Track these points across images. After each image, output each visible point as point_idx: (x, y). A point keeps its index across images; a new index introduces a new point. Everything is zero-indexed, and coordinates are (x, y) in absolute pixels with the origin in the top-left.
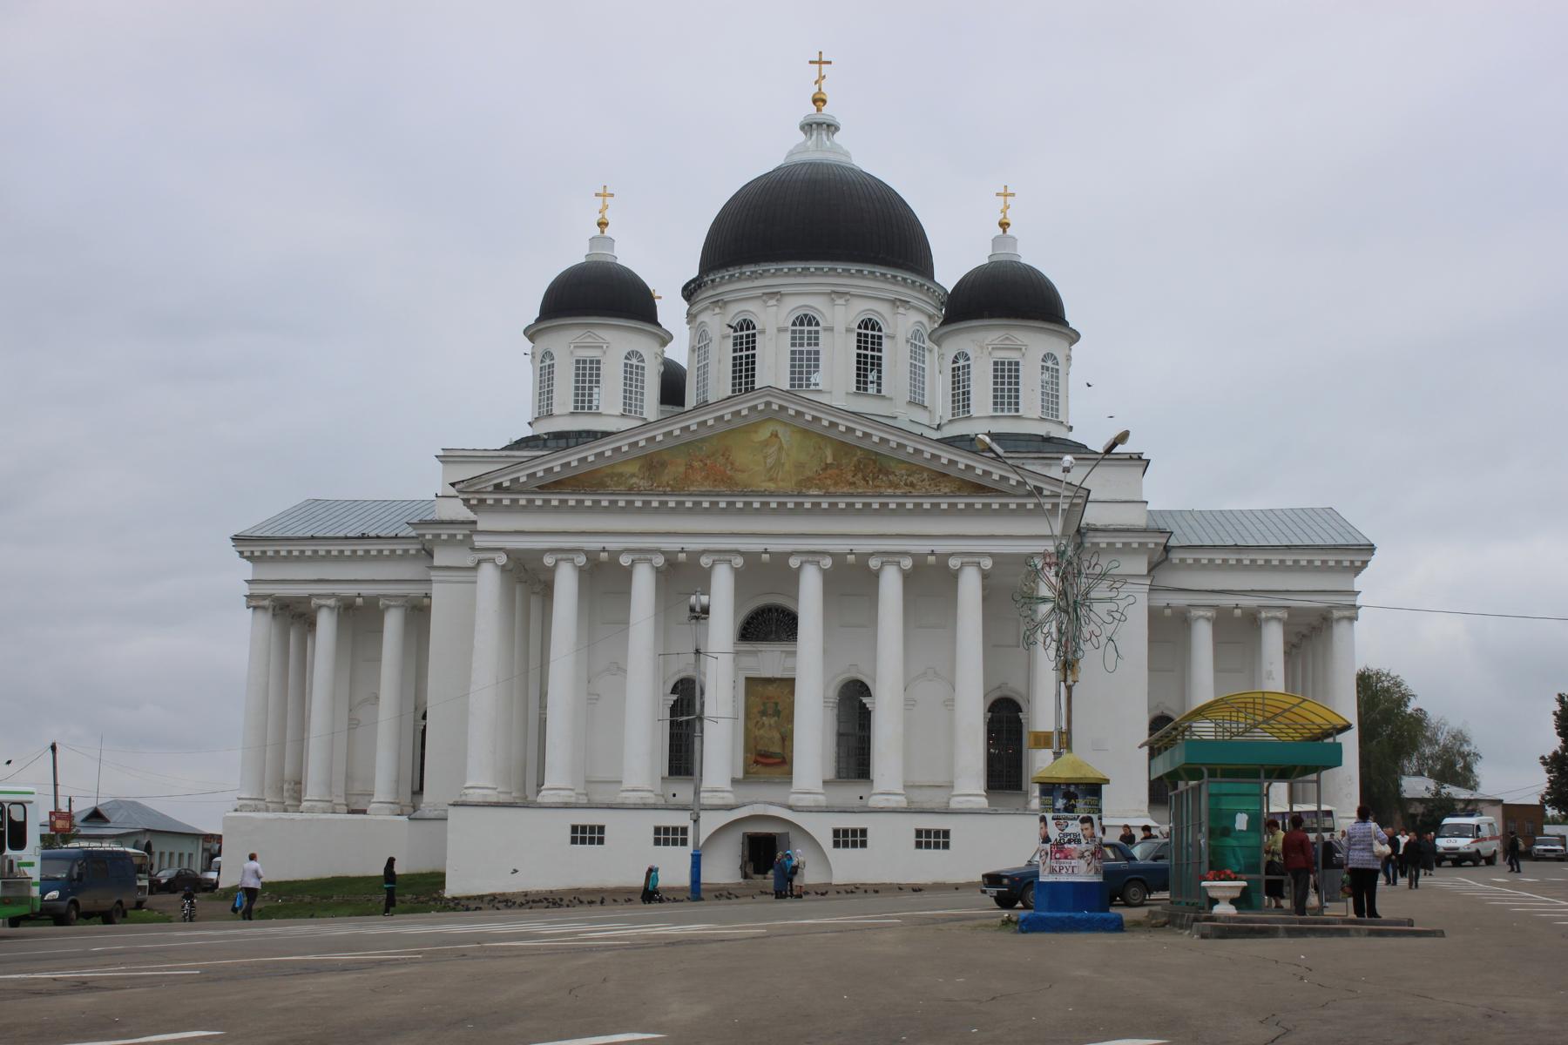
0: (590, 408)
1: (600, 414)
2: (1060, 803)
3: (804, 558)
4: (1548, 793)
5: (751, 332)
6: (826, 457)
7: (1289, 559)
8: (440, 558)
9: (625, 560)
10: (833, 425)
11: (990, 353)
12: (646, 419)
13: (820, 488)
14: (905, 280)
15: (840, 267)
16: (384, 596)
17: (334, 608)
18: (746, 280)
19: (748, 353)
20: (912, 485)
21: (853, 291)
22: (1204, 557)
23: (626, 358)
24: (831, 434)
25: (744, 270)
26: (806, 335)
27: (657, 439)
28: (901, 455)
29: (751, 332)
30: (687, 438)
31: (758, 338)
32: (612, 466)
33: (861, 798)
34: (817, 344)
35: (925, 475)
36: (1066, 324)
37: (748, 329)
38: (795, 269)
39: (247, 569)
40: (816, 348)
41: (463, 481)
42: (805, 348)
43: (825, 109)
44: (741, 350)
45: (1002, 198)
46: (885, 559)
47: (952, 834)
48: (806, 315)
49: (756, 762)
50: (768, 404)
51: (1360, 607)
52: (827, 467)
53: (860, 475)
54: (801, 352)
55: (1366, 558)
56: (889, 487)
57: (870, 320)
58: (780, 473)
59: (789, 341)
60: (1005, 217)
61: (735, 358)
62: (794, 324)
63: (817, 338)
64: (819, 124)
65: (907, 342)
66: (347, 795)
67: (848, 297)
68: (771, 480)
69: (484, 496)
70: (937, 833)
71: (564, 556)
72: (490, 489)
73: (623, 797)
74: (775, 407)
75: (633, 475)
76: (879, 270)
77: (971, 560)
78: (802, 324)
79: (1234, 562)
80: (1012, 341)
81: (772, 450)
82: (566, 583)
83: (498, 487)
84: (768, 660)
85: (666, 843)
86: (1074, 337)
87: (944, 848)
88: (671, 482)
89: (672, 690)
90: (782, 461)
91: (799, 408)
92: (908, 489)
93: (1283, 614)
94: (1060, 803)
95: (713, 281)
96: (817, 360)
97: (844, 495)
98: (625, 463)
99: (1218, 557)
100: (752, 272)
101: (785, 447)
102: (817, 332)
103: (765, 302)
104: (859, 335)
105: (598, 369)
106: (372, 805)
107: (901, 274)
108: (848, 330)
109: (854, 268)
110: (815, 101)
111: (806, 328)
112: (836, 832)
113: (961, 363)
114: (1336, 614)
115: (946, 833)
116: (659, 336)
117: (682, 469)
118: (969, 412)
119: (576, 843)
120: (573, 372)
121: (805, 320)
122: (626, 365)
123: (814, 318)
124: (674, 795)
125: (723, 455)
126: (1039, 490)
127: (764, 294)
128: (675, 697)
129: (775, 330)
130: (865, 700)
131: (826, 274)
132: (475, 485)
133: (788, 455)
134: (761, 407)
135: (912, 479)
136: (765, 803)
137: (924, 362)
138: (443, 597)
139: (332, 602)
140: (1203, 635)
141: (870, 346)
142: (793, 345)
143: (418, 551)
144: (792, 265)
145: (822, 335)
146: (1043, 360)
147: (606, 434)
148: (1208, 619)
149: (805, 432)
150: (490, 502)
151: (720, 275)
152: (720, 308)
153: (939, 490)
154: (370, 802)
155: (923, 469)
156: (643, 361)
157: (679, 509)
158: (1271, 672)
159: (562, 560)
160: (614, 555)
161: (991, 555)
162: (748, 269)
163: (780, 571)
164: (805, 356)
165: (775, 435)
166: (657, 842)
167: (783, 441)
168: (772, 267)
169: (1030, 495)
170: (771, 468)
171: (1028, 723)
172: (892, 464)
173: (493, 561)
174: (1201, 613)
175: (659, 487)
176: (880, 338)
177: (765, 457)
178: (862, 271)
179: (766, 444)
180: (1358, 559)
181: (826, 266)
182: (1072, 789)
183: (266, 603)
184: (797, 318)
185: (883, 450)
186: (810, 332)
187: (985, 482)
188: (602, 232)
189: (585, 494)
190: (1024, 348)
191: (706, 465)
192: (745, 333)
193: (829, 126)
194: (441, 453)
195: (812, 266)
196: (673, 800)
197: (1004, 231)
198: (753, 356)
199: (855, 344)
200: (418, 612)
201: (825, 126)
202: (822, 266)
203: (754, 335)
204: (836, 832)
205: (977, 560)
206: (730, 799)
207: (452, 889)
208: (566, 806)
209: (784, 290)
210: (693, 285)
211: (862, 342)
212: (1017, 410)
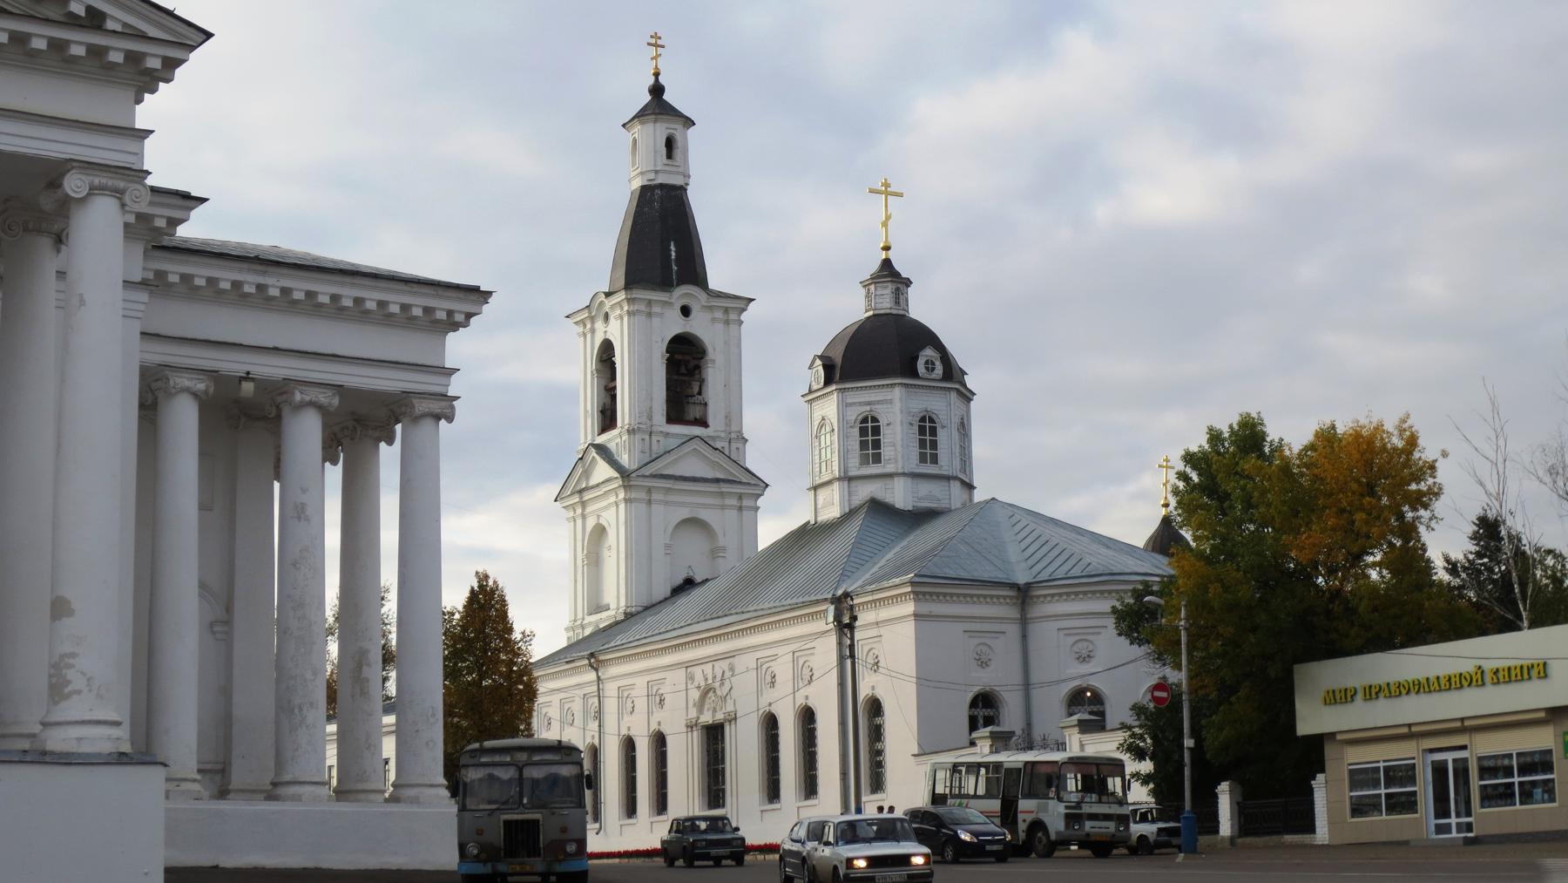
79: (252, 290)
93: (332, 400)
99: (226, 276)
114: (421, 406)
148: (195, 395)
158: (303, 505)
169: (73, 21)
174: (184, 381)
180: (460, 306)
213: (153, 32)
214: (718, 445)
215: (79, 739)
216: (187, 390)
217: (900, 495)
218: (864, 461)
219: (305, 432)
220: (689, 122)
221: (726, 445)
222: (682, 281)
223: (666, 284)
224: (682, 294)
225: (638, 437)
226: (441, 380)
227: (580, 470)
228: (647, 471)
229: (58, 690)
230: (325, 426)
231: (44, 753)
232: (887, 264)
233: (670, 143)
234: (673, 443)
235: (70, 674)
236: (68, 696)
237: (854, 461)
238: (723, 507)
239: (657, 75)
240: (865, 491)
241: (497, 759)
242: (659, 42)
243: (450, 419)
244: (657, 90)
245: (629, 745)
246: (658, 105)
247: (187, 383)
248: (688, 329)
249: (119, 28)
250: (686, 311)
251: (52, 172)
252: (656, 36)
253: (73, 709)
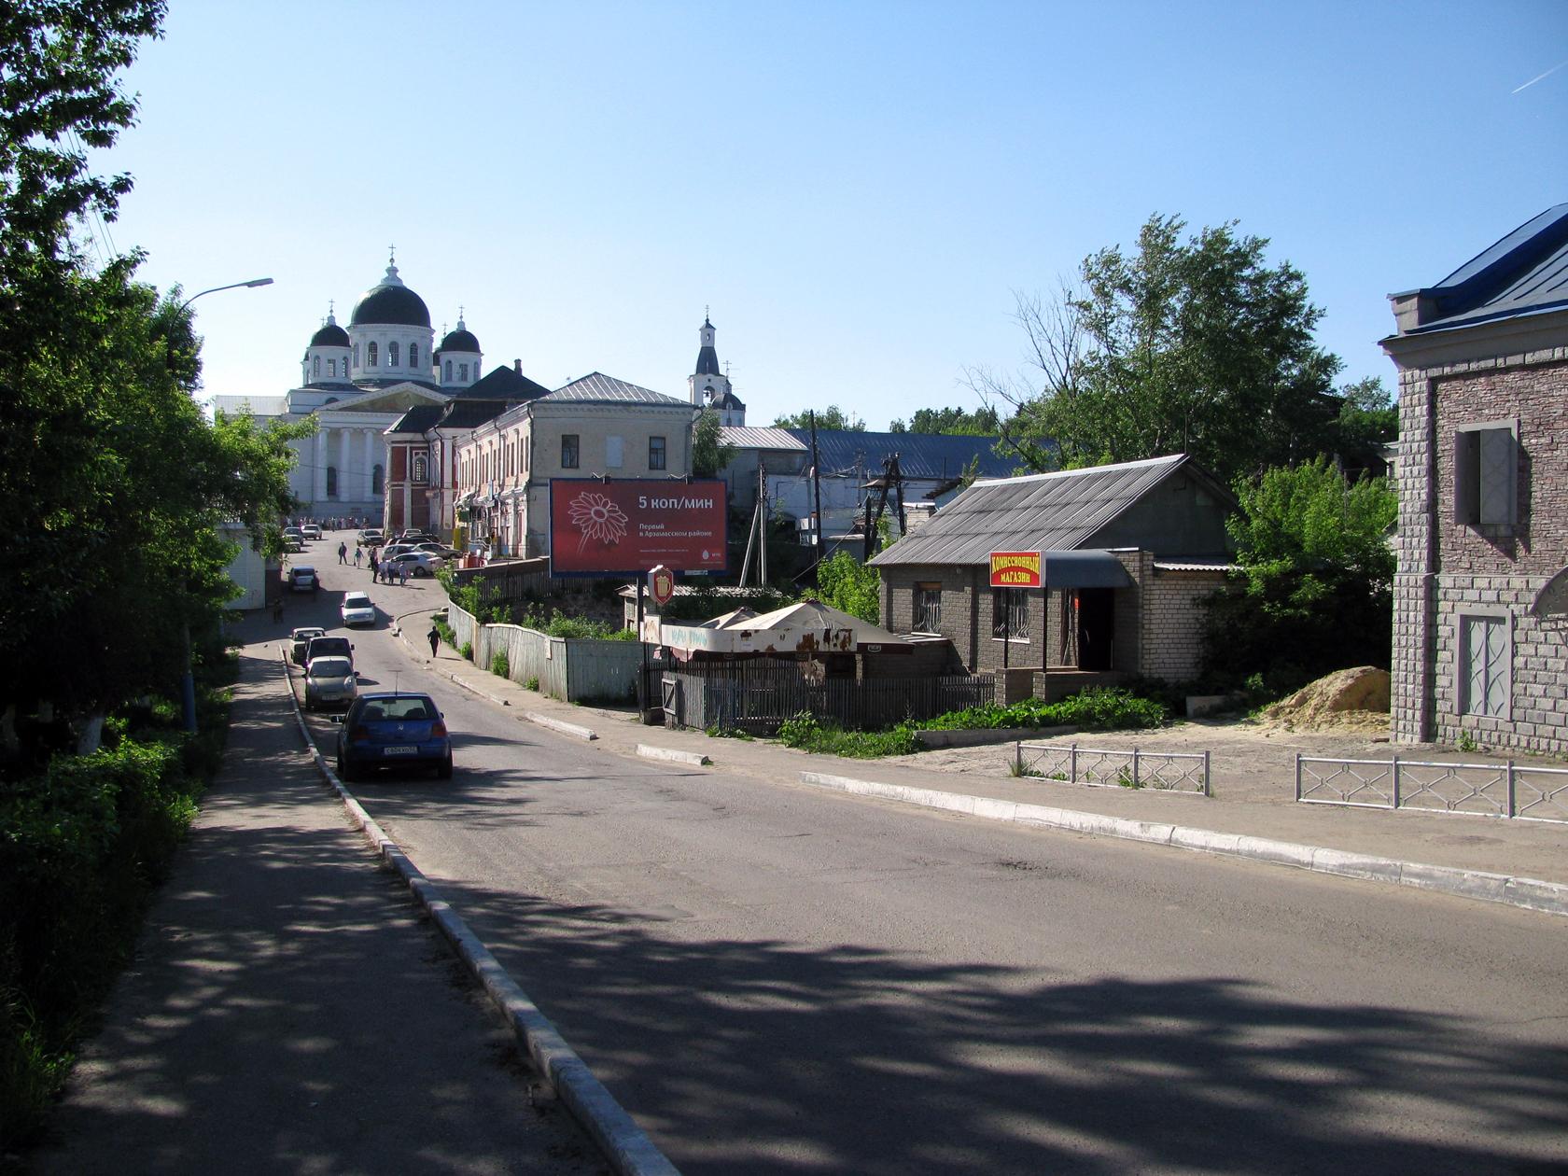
73: (365, 500)
81: (407, 399)
149: (417, 395)
160: (362, 430)
168: (383, 325)
244: (707, 320)
246: (708, 325)
250: (709, 380)
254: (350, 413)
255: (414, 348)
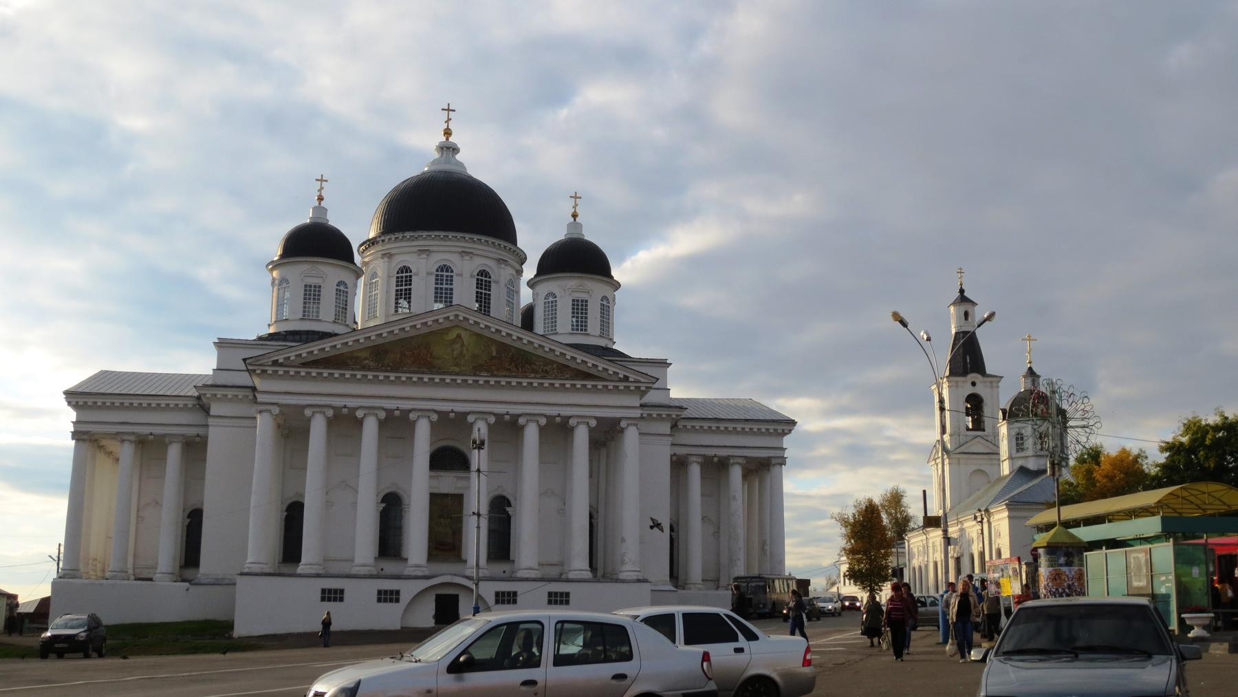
0: (309, 316)
1: (320, 320)
2: (1062, 560)
3: (477, 416)
4: (847, 571)
5: (408, 274)
6: (492, 352)
7: (747, 427)
8: (214, 410)
9: (359, 414)
10: (498, 331)
11: (570, 294)
12: (348, 325)
13: (488, 373)
14: (505, 247)
15: (468, 236)
16: (168, 434)
17: (133, 442)
18: (406, 241)
19: (406, 287)
20: (547, 372)
21: (476, 252)
22: (697, 424)
23: (337, 285)
24: (497, 337)
25: (405, 235)
26: (445, 278)
27: (383, 336)
28: (540, 352)
29: (408, 274)
30: (403, 335)
31: (413, 278)
32: (352, 352)
33: (504, 572)
34: (451, 284)
35: (555, 366)
36: (612, 277)
37: (407, 272)
38: (439, 236)
39: (72, 415)
40: (451, 287)
41: (251, 358)
42: (444, 286)
43: (451, 139)
44: (402, 285)
45: (573, 199)
46: (529, 418)
47: (571, 596)
48: (445, 266)
49: (437, 548)
50: (457, 316)
51: (786, 458)
52: (492, 358)
53: (513, 365)
54: (441, 289)
55: (789, 428)
56: (532, 373)
57: (484, 271)
58: (462, 361)
59: (434, 281)
60: (575, 211)
61: (397, 291)
62: (437, 271)
63: (452, 280)
64: (448, 148)
65: (506, 285)
66: (134, 568)
67: (471, 255)
68: (457, 365)
69: (266, 368)
70: (562, 594)
71: (318, 410)
72: (270, 363)
73: (355, 571)
74: (461, 318)
75: (366, 359)
76: (491, 240)
77: (583, 420)
78: (442, 271)
80: (583, 286)
81: (457, 346)
82: (318, 428)
83: (275, 363)
84: (448, 483)
85: (385, 601)
86: (617, 286)
87: (513, 603)
88: (391, 364)
89: (382, 499)
90: (464, 353)
91: (477, 320)
92: (545, 375)
94: (1062, 560)
95: (383, 241)
96: (451, 294)
97: (506, 376)
98: (361, 350)
100: (411, 236)
101: (465, 343)
102: (452, 276)
103: (419, 255)
104: (478, 279)
105: (319, 291)
106: (158, 575)
107: (503, 243)
108: (472, 276)
109: (476, 237)
110: (445, 134)
111: (445, 274)
112: (497, 594)
113: (551, 299)
115: (568, 594)
116: (356, 272)
117: (398, 356)
118: (555, 330)
119: (325, 601)
120: (303, 292)
121: (445, 268)
122: (337, 290)
123: (450, 267)
124: (382, 570)
125: (426, 348)
126: (626, 379)
127: (419, 250)
128: (384, 505)
129: (425, 273)
130: (508, 509)
131: (458, 240)
132: (259, 360)
133: (467, 350)
134: (452, 318)
135: (548, 368)
136: (451, 574)
137: (513, 300)
138: (218, 438)
139: (132, 438)
140: (695, 471)
141: (484, 287)
142: (436, 284)
143: (194, 405)
144: (437, 233)
145: (455, 278)
146: (601, 300)
147: (336, 335)
148: (698, 463)
149: (479, 336)
150: (269, 372)
151: (388, 237)
152: (388, 258)
153: (564, 376)
154: (155, 574)
155: (553, 362)
156: (347, 288)
157: (398, 381)
159: (317, 412)
161: (596, 418)
162: (408, 234)
163: (459, 422)
164: (444, 291)
165: (459, 336)
166: (379, 600)
167: (464, 340)
168: (425, 234)
169: (620, 380)
170: (456, 358)
171: (597, 525)
172: (534, 358)
173: (270, 411)
174: (694, 459)
175: (382, 366)
176: (490, 282)
177: (453, 351)
178: (480, 240)
179: (453, 342)
180: (786, 428)
181: (459, 235)
182: (1070, 550)
183: (86, 437)
184: (439, 267)
185: (528, 349)
186: (447, 276)
187: (593, 372)
188: (320, 204)
189: (335, 369)
190: (591, 292)
191: (414, 353)
192: (404, 275)
193: (453, 149)
194: (217, 341)
195: (450, 235)
196: (383, 573)
197: (575, 220)
198: (410, 289)
199: (412, 292)
200: (195, 448)
201: (451, 149)
202: (457, 235)
203: (411, 276)
204: (497, 594)
205: (587, 420)
206: (426, 572)
207: (240, 630)
208: (318, 576)
209: (431, 249)
210: (368, 243)
211: (479, 284)
212: (586, 330)
213: (643, 380)
214: (989, 439)
215: (627, 576)
216: (696, 461)
217: (1032, 465)
218: (1018, 451)
219: (736, 473)
220: (974, 304)
221: (992, 438)
222: (972, 371)
223: (965, 373)
224: (973, 376)
225: (954, 437)
226: (781, 452)
227: (934, 451)
228: (958, 451)
229: (623, 563)
230: (743, 468)
231: (619, 579)
232: (1030, 369)
233: (966, 314)
234: (969, 438)
235: (625, 558)
236: (624, 564)
237: (1014, 451)
238: (992, 464)
239: (961, 285)
240: (1019, 463)
241: (742, 580)
242: (962, 271)
243: (785, 465)
244: (962, 291)
245: (936, 564)
246: (963, 299)
247: (695, 459)
248: (974, 391)
249: (633, 380)
250: (974, 384)
251: (619, 420)
252: (961, 269)
253: (627, 567)
254: (326, 373)
255: (483, 281)
